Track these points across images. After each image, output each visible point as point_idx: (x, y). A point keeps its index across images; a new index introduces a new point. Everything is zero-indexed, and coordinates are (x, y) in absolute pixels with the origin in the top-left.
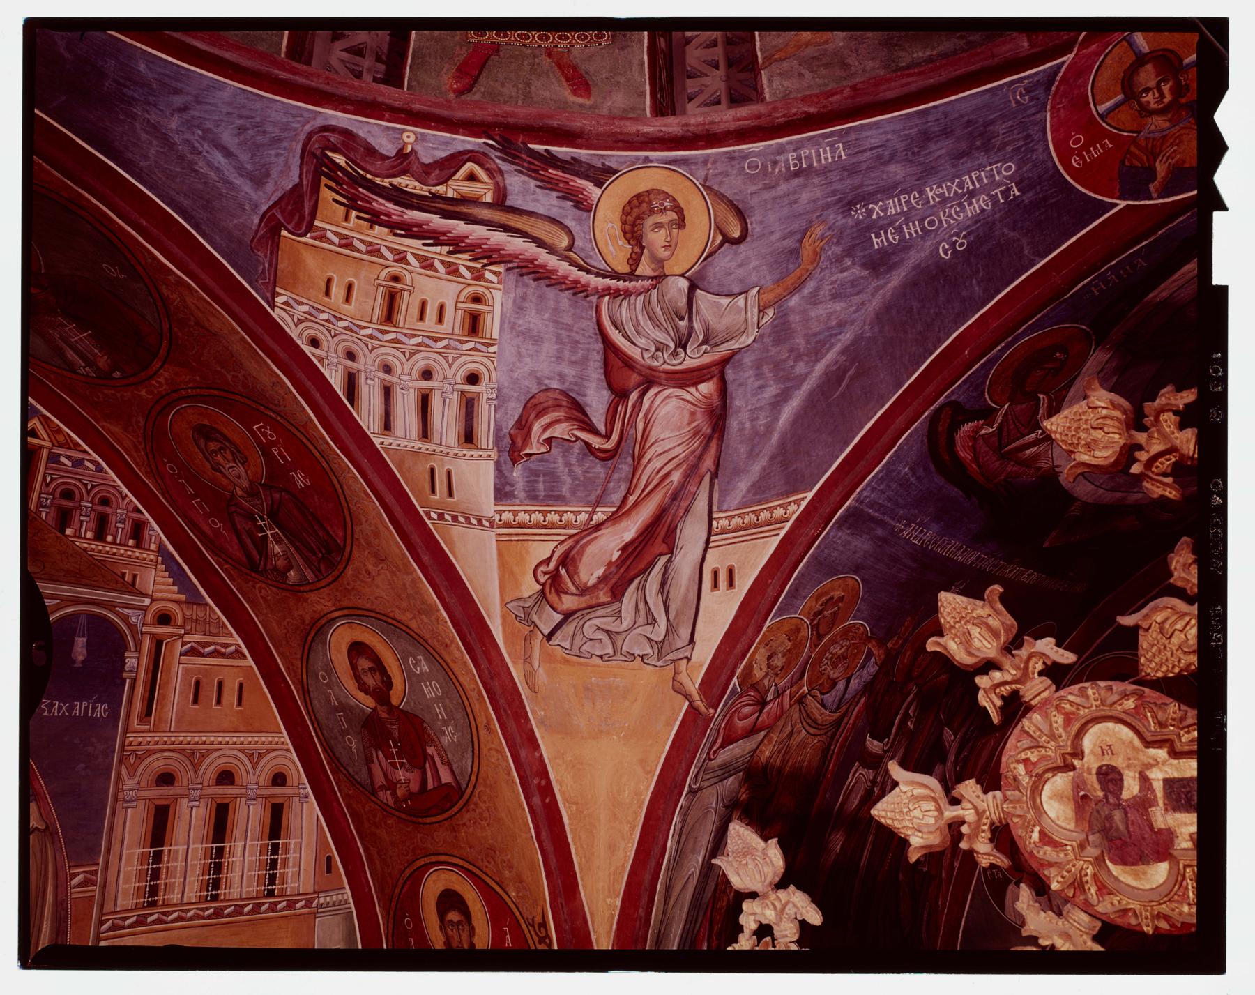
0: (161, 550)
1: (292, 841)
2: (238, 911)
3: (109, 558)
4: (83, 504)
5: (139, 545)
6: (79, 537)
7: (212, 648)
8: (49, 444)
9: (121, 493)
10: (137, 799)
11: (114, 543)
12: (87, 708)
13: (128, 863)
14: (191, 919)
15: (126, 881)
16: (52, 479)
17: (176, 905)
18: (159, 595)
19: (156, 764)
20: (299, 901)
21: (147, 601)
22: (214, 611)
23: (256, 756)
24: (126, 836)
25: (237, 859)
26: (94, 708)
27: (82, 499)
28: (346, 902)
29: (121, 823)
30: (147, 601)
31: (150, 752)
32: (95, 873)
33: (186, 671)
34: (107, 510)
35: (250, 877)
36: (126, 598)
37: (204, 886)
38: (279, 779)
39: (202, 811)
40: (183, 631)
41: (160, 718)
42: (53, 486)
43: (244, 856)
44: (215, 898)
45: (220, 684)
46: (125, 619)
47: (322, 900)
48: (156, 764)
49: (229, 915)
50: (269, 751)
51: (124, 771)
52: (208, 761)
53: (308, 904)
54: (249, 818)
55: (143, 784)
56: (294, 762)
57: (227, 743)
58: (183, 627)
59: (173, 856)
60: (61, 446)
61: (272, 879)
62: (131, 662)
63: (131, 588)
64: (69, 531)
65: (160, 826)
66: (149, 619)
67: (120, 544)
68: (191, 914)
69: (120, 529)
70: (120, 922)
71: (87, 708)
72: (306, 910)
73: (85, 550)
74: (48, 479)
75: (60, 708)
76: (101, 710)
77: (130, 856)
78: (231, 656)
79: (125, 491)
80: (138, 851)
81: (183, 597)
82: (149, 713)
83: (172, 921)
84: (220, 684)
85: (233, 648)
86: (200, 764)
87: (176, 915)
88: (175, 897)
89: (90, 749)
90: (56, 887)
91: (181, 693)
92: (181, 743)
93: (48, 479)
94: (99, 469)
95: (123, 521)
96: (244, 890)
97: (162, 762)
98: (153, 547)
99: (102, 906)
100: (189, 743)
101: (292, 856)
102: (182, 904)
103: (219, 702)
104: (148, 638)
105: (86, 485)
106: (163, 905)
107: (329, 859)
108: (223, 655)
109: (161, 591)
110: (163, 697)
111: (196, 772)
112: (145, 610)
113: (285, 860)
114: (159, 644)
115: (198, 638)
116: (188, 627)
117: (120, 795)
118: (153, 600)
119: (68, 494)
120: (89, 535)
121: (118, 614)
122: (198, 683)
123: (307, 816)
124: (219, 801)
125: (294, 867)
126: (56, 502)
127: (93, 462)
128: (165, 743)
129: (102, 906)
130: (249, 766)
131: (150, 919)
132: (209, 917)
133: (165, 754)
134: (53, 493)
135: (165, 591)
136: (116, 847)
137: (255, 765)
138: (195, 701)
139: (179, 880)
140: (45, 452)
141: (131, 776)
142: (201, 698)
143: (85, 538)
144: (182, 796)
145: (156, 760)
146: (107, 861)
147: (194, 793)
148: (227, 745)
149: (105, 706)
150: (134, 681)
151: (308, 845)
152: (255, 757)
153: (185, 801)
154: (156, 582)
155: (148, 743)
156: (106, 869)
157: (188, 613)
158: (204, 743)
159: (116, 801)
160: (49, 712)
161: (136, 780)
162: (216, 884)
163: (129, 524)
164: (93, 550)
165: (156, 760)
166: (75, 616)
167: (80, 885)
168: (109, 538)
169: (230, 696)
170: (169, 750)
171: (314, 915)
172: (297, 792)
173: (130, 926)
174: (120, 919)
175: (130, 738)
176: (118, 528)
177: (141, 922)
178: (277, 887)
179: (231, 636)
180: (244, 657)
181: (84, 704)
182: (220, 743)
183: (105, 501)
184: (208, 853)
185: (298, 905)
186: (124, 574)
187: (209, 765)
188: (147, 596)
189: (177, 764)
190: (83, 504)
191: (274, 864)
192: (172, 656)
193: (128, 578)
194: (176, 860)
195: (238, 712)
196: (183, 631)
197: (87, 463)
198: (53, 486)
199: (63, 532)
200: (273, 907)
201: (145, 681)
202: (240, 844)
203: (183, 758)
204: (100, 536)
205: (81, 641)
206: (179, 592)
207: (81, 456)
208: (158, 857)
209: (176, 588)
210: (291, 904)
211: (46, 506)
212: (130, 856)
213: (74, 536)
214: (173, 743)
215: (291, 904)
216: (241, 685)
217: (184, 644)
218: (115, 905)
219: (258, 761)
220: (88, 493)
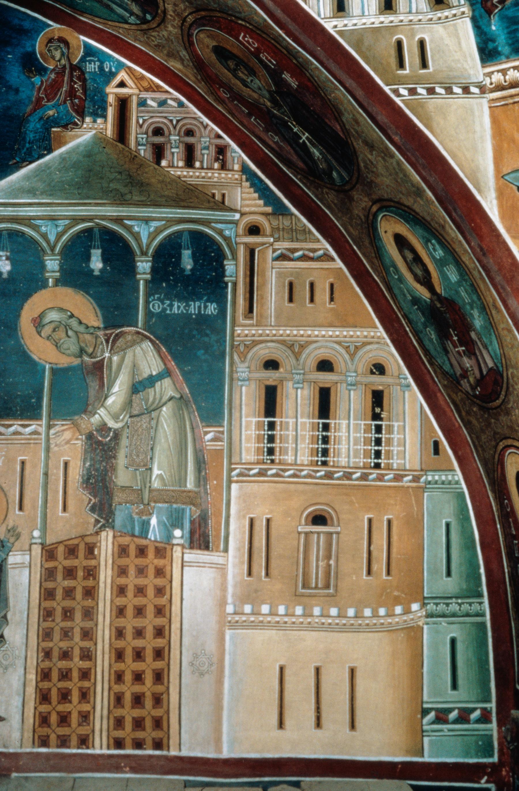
0: (245, 169)
1: (396, 424)
2: (348, 476)
3: (199, 182)
4: (172, 138)
5: (223, 167)
6: (173, 167)
7: (300, 253)
8: (136, 91)
9: (202, 123)
10: (249, 380)
11: (202, 168)
12: (200, 307)
13: (248, 428)
14: (305, 477)
15: (248, 440)
16: (144, 121)
17: (291, 465)
18: (247, 209)
19: (262, 352)
20: (406, 475)
21: (237, 216)
22: (299, 220)
23: (352, 349)
24: (243, 407)
25: (343, 433)
26: (206, 307)
27: (170, 134)
28: (457, 483)
29: (238, 397)
30: (237, 216)
31: (255, 343)
32: (222, 433)
33: (280, 275)
34: (190, 140)
35: (356, 451)
36: (218, 215)
37: (314, 452)
38: (379, 369)
39: (306, 392)
40: (272, 240)
41: (261, 316)
42: (145, 126)
43: (350, 432)
44: (324, 463)
45: (312, 285)
46: (220, 232)
47: (430, 478)
48: (264, 352)
49: (339, 479)
50: (365, 344)
51: (236, 357)
52: (307, 351)
53: (416, 479)
54: (351, 403)
55: (253, 368)
56: (393, 355)
57: (324, 336)
58: (272, 236)
59: (285, 426)
60: (147, 90)
61: (378, 454)
62: (229, 267)
63: (221, 205)
64: (164, 163)
65: (270, 402)
66: (241, 231)
67: (207, 169)
68: (304, 473)
69: (205, 155)
70: (246, 472)
71: (200, 307)
72: (414, 484)
73: (179, 177)
74: (141, 121)
75: (179, 307)
76: (212, 309)
77: (248, 424)
78: (319, 259)
79: (206, 120)
80: (254, 420)
81: (269, 209)
82: (251, 310)
83: (289, 477)
84: (312, 285)
85: (321, 252)
86: (300, 353)
87: (291, 472)
88: (289, 458)
89: (206, 339)
90: (194, 440)
91: (276, 293)
92: (281, 335)
93: (141, 121)
94: (181, 105)
95: (207, 148)
96: (352, 460)
97: (267, 351)
98: (236, 167)
99: (230, 457)
100: (288, 336)
101: (396, 436)
102: (296, 464)
103: (312, 300)
104: (242, 247)
105: (171, 121)
106: (280, 463)
107: (436, 444)
108: (312, 259)
109: (248, 206)
110: (262, 297)
111: (297, 360)
112: (236, 223)
113: (389, 442)
114: (252, 253)
115: (287, 245)
116: (276, 236)
117: (235, 376)
118: (242, 214)
119: (158, 132)
120: (181, 164)
121: (214, 229)
122: (291, 285)
123: (410, 404)
124: (322, 385)
125: (399, 445)
126: (149, 139)
127: (175, 100)
128: (268, 335)
129: (230, 457)
130: (347, 357)
131: (270, 473)
132: (321, 478)
133: (269, 344)
134: (146, 133)
135: (252, 206)
136: (236, 414)
137: (352, 356)
138: (291, 300)
139: (291, 446)
140: (135, 99)
141: (243, 362)
142: (295, 297)
143: (177, 167)
144: (286, 379)
145: (261, 349)
146: (230, 423)
147: (297, 377)
148: (325, 338)
149: (214, 305)
150: (235, 284)
151: (412, 428)
152: (353, 350)
153: (290, 384)
154: (245, 200)
155: (254, 335)
156: (230, 431)
157: (275, 223)
158: (302, 336)
159: (232, 379)
160: (171, 310)
161: (246, 364)
162: (325, 452)
163: (213, 150)
164: (185, 177)
165: (261, 349)
166: (179, 234)
167: (212, 440)
168: (197, 164)
169: (323, 294)
170: (272, 341)
171: (423, 489)
172: (397, 381)
173: (254, 475)
174: (246, 469)
175: (238, 330)
176: (203, 155)
177: (262, 473)
178: (383, 461)
179: (318, 241)
180: (333, 259)
181: (197, 304)
182: (317, 336)
183: (189, 133)
184: (314, 427)
185: (406, 479)
186: (214, 195)
187: (309, 354)
188: (236, 211)
189: (279, 352)
190: (172, 138)
191: (378, 442)
192: (265, 260)
193: (218, 197)
194: (287, 429)
195: (332, 309)
196: (272, 240)
197: (170, 102)
198: (145, 126)
199: (158, 163)
200: (380, 478)
201: (245, 283)
202: (344, 423)
203: (285, 348)
204: (189, 162)
205: (187, 255)
206: (265, 205)
207: (164, 96)
208: (272, 426)
209: (261, 202)
210: (398, 478)
211: (143, 145)
212: (248, 424)
213: (169, 166)
214: (275, 335)
215: (398, 478)
216: (332, 286)
217: (274, 251)
218: (241, 459)
219: (355, 353)
220: (175, 128)
